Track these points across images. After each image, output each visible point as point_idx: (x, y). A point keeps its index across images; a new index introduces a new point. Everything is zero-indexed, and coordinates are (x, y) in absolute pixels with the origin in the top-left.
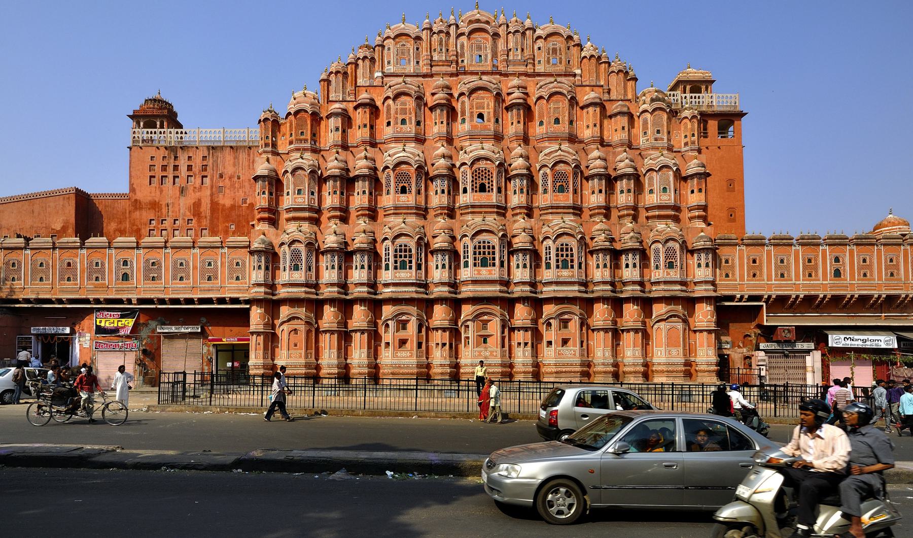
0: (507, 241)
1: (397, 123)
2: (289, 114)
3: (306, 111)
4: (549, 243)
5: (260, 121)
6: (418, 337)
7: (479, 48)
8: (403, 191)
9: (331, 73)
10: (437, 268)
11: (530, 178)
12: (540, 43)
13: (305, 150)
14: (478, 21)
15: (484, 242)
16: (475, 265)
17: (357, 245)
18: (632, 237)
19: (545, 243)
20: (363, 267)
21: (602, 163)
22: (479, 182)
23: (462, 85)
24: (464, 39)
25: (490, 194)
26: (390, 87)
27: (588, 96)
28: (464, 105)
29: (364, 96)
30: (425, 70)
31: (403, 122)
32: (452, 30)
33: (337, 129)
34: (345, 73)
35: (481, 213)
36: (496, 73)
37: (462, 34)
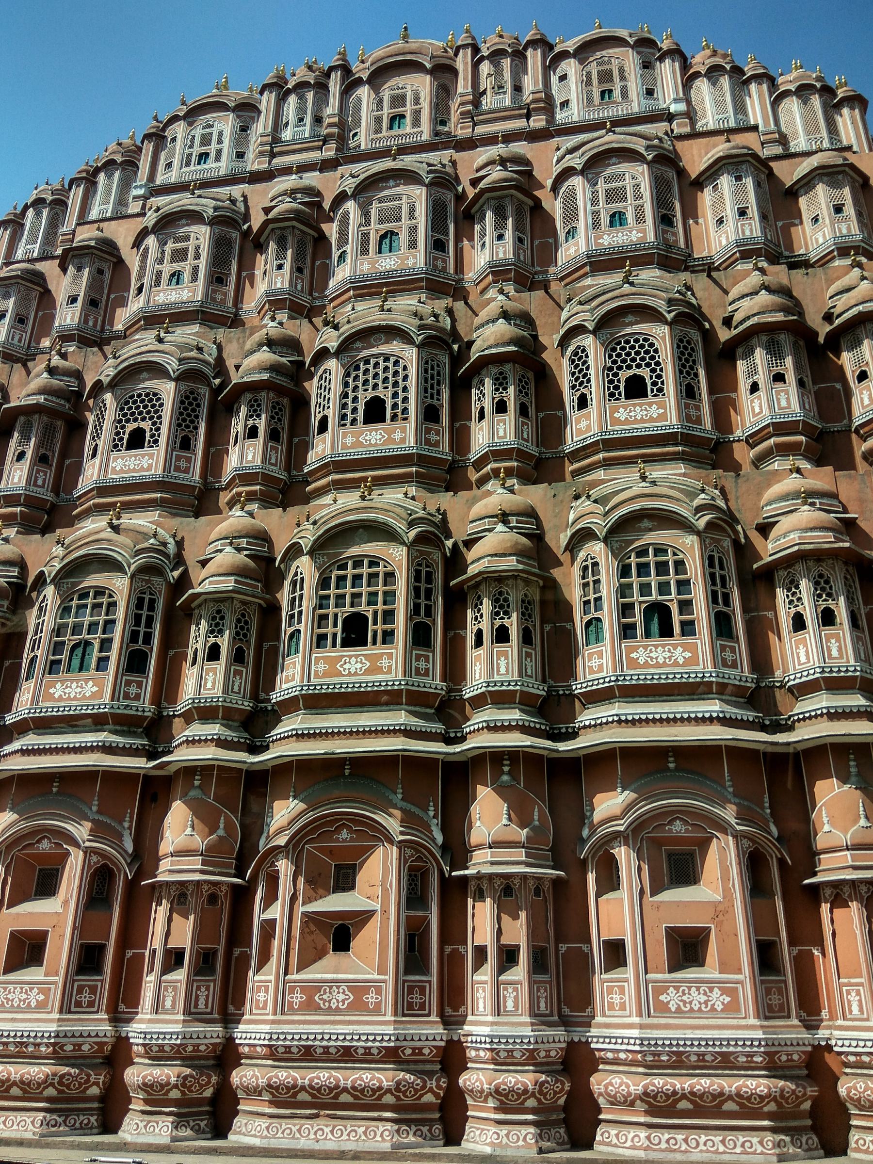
1: (158, 284)
6: (82, 927)
8: (137, 441)
16: (320, 641)
22: (364, 396)
24: (364, 93)
25: (400, 423)
36: (445, 146)
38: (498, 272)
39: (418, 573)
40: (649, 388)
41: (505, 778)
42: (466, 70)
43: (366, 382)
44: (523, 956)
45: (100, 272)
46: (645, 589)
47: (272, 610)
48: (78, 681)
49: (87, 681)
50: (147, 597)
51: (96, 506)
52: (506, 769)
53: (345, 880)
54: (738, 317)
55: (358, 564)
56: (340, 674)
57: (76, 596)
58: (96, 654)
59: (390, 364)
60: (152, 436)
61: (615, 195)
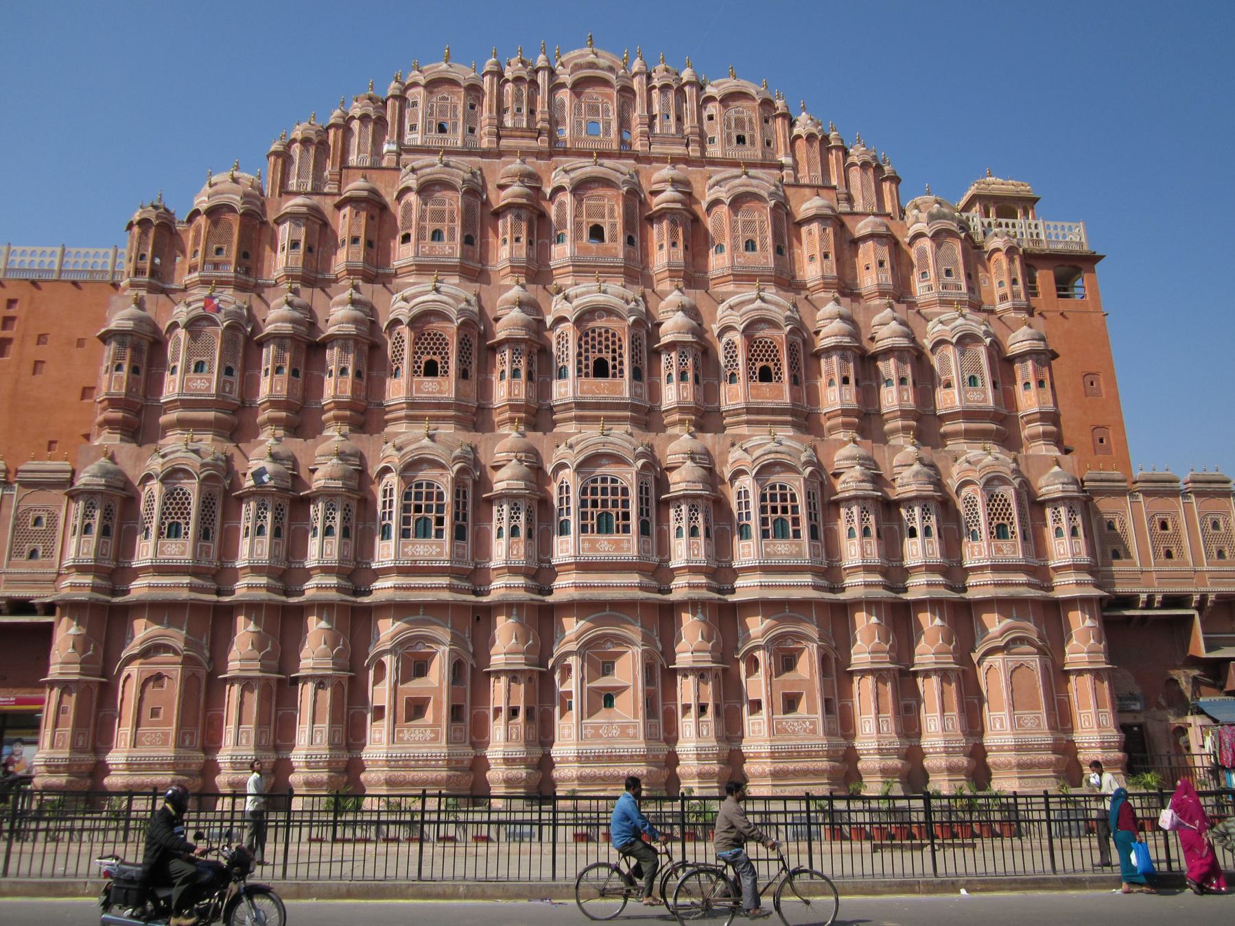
0: (655, 475)
3: (231, 209)
4: (747, 482)
5: (130, 226)
6: (453, 694)
7: (594, 110)
8: (431, 370)
10: (500, 535)
13: (222, 283)
14: (592, 65)
15: (604, 480)
16: (584, 529)
17: (318, 482)
18: (916, 474)
21: (845, 327)
22: (593, 356)
23: (557, 176)
24: (564, 95)
25: (618, 380)
27: (808, 205)
28: (563, 209)
29: (355, 186)
30: (485, 143)
31: (437, 235)
32: (542, 78)
33: (295, 245)
34: (322, 147)
35: (596, 419)
36: (628, 156)
37: (563, 85)
38: (673, 273)
41: (700, 615)
43: (593, 347)
44: (710, 709)
45: (372, 218)
46: (774, 510)
47: (544, 503)
51: (408, 417)
53: (607, 669)
54: (821, 335)
55: (604, 480)
56: (598, 550)
58: (434, 528)
61: (748, 225)
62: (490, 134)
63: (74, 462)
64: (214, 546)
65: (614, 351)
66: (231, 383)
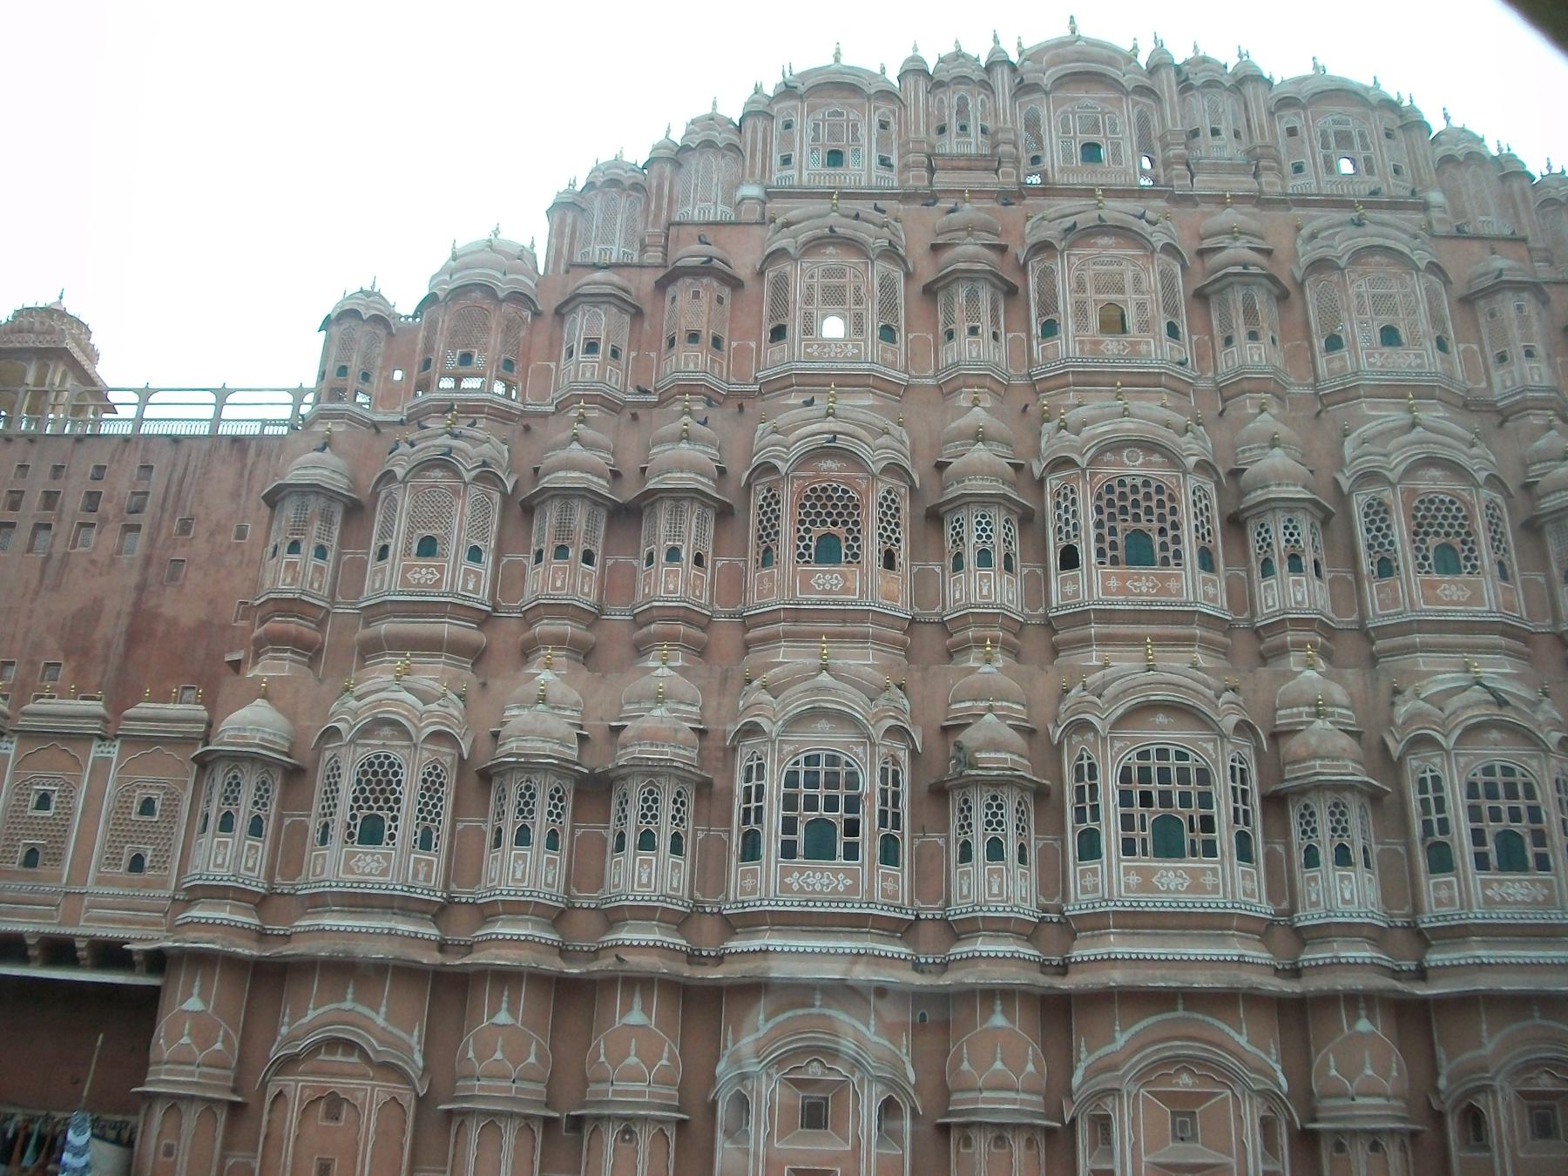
2: (430, 300)
5: (327, 324)
8: (828, 551)
9: (590, 185)
10: (966, 854)
11: (1329, 515)
12: (1290, 118)
15: (1162, 754)
16: (1128, 847)
19: (1412, 763)
20: (647, 842)
25: (1172, 570)
26: (787, 225)
32: (1002, 80)
35: (1137, 641)
37: (1034, 88)
39: (1232, 768)
40: (1463, 562)
42: (1171, 97)
45: (720, 300)
48: (822, 871)
49: (835, 872)
50: (890, 768)
52: (1363, 1013)
56: (1157, 890)
57: (801, 758)
59: (1152, 490)
60: (849, 547)
62: (917, 165)
63: (211, 708)
64: (437, 859)
65: (1162, 518)
66: (478, 575)
